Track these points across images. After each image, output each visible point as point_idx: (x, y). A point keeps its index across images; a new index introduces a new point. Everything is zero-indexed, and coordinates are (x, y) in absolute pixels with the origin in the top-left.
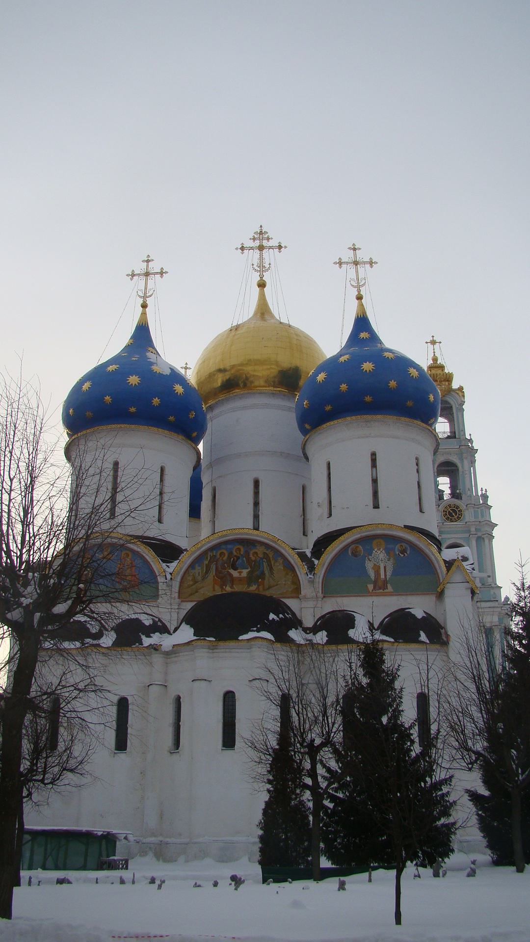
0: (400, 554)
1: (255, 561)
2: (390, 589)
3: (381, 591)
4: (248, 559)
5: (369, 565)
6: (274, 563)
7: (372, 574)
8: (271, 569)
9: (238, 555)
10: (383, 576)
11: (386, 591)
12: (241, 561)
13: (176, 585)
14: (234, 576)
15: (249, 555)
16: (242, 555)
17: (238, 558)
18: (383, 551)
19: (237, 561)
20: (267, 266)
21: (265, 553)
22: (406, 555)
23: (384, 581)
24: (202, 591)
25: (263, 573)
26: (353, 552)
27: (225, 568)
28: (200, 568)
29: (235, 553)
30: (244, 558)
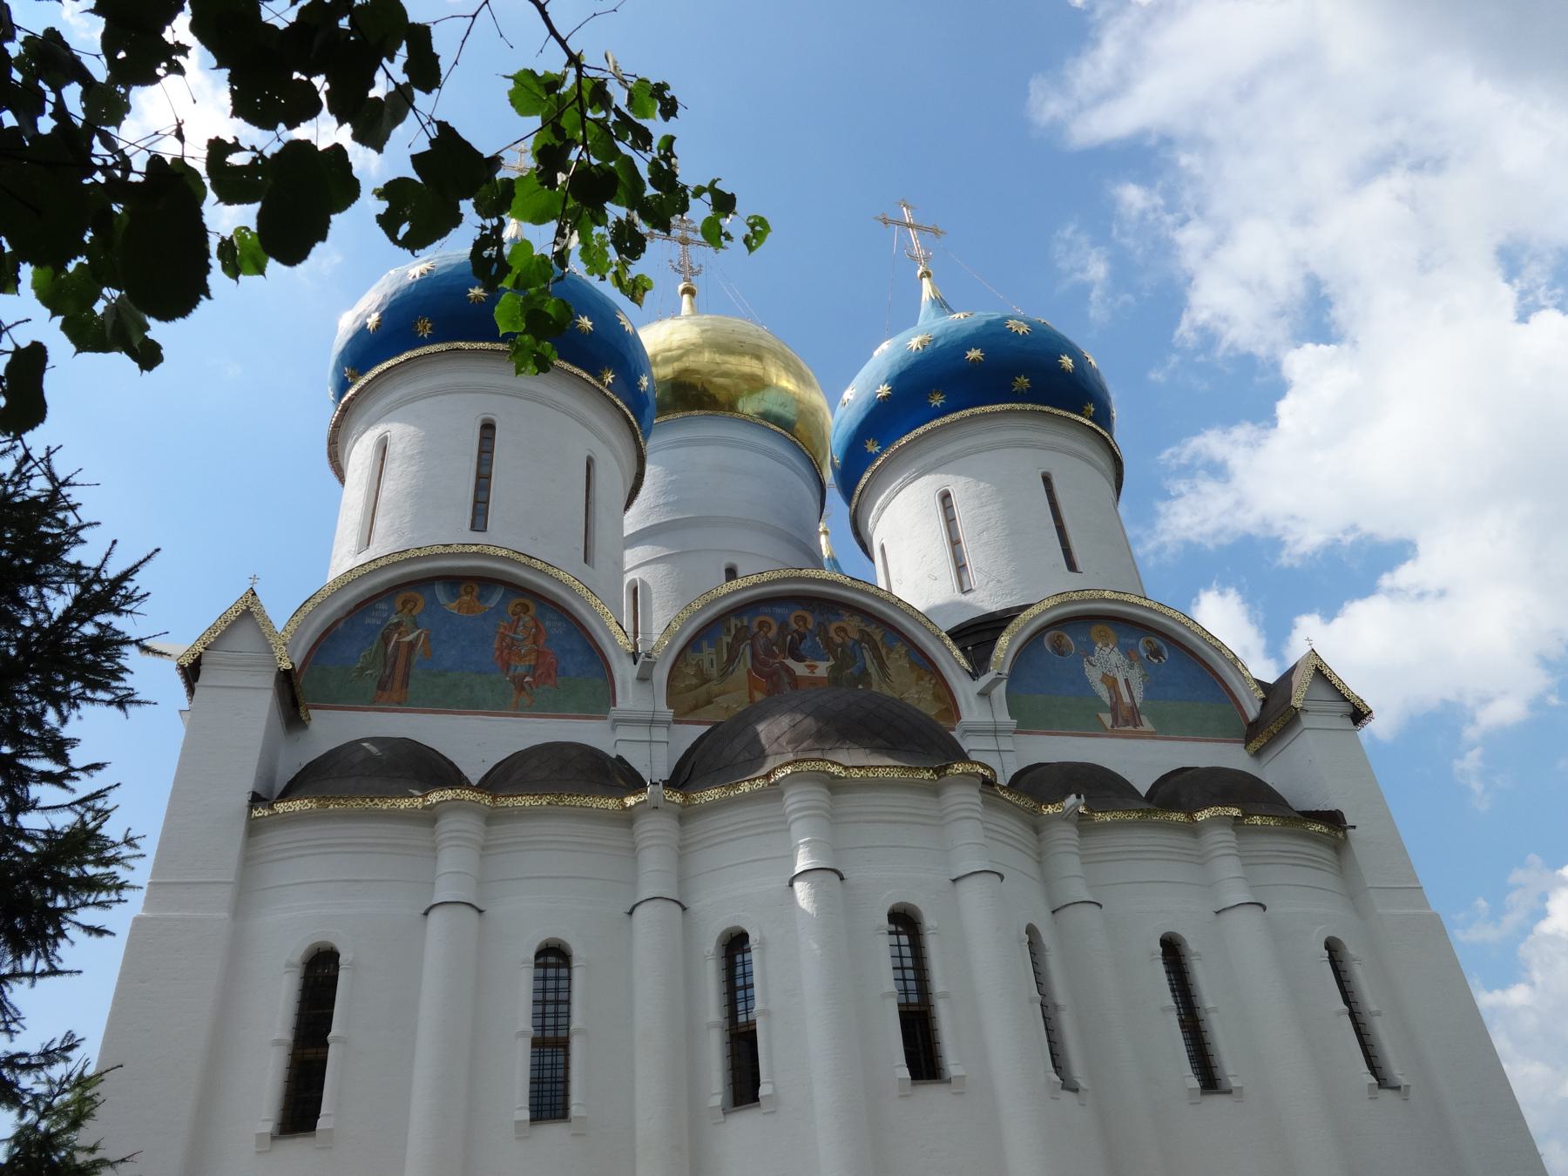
0: (1152, 659)
1: (842, 645)
2: (1147, 725)
3: (1130, 728)
4: (828, 642)
5: (1094, 675)
6: (888, 654)
7: (1103, 693)
8: (882, 666)
9: (802, 630)
10: (1126, 699)
11: (1140, 728)
12: (809, 644)
13: (661, 674)
14: (797, 674)
15: (827, 632)
16: (810, 631)
17: (803, 637)
18: (1116, 649)
19: (800, 643)
20: (696, 269)
21: (861, 631)
22: (1164, 661)
23: (1132, 708)
24: (722, 701)
25: (864, 672)
26: (1053, 646)
27: (774, 656)
28: (713, 650)
29: (795, 626)
30: (817, 638)
